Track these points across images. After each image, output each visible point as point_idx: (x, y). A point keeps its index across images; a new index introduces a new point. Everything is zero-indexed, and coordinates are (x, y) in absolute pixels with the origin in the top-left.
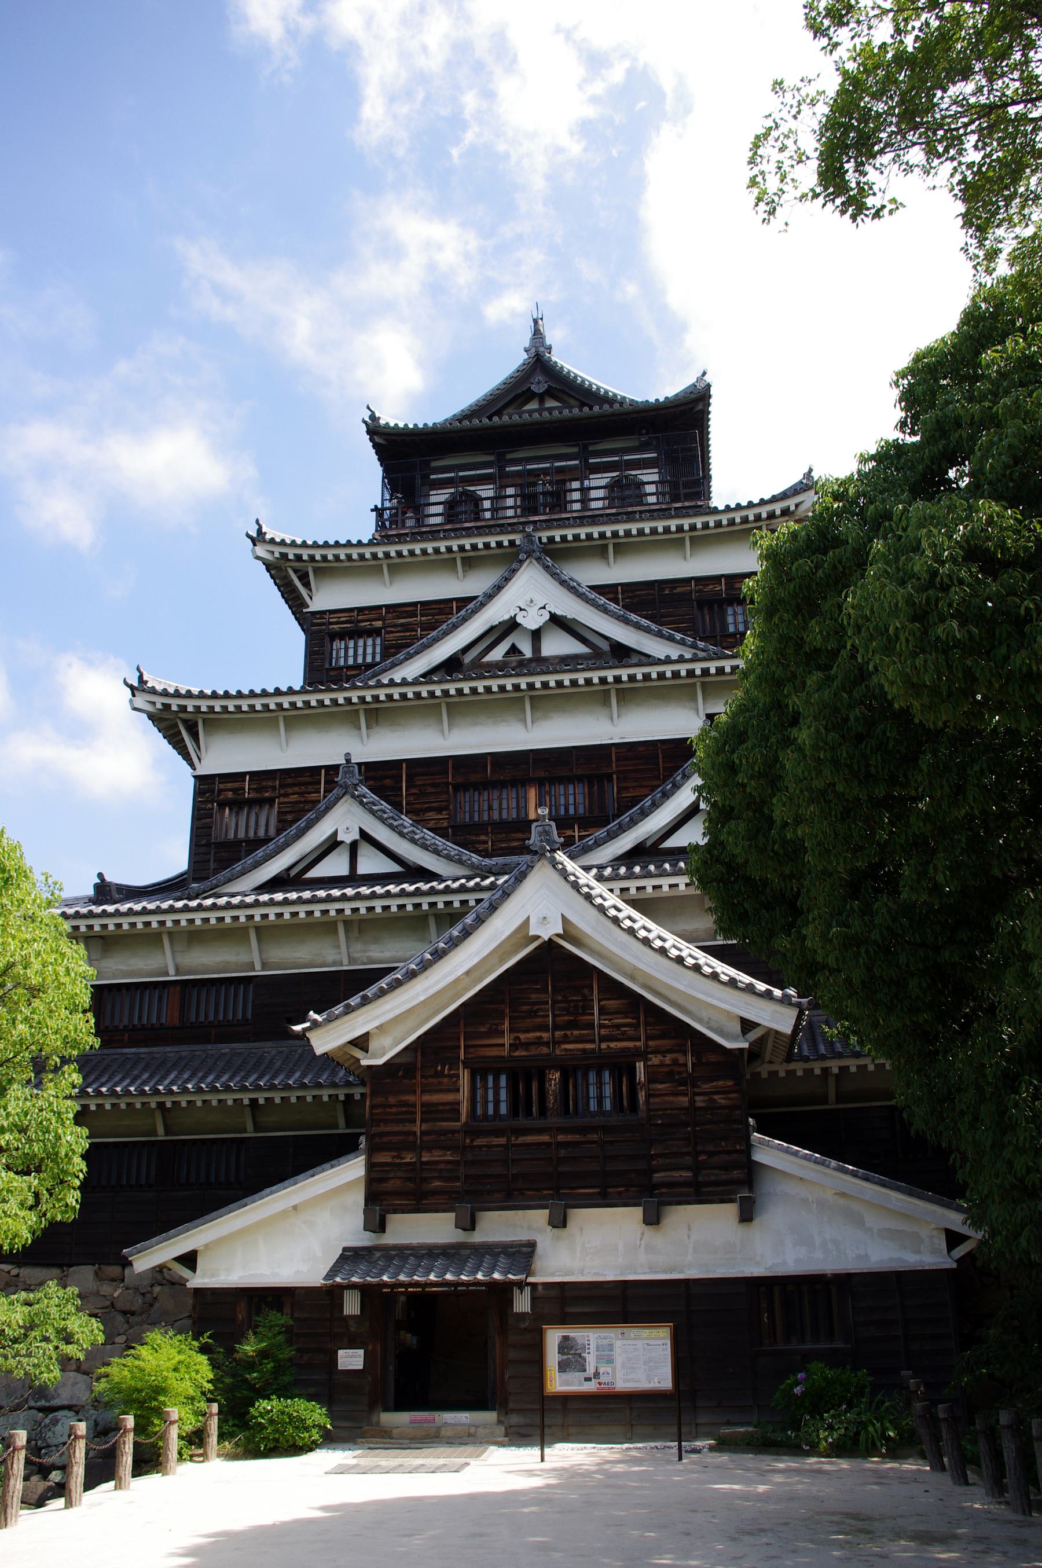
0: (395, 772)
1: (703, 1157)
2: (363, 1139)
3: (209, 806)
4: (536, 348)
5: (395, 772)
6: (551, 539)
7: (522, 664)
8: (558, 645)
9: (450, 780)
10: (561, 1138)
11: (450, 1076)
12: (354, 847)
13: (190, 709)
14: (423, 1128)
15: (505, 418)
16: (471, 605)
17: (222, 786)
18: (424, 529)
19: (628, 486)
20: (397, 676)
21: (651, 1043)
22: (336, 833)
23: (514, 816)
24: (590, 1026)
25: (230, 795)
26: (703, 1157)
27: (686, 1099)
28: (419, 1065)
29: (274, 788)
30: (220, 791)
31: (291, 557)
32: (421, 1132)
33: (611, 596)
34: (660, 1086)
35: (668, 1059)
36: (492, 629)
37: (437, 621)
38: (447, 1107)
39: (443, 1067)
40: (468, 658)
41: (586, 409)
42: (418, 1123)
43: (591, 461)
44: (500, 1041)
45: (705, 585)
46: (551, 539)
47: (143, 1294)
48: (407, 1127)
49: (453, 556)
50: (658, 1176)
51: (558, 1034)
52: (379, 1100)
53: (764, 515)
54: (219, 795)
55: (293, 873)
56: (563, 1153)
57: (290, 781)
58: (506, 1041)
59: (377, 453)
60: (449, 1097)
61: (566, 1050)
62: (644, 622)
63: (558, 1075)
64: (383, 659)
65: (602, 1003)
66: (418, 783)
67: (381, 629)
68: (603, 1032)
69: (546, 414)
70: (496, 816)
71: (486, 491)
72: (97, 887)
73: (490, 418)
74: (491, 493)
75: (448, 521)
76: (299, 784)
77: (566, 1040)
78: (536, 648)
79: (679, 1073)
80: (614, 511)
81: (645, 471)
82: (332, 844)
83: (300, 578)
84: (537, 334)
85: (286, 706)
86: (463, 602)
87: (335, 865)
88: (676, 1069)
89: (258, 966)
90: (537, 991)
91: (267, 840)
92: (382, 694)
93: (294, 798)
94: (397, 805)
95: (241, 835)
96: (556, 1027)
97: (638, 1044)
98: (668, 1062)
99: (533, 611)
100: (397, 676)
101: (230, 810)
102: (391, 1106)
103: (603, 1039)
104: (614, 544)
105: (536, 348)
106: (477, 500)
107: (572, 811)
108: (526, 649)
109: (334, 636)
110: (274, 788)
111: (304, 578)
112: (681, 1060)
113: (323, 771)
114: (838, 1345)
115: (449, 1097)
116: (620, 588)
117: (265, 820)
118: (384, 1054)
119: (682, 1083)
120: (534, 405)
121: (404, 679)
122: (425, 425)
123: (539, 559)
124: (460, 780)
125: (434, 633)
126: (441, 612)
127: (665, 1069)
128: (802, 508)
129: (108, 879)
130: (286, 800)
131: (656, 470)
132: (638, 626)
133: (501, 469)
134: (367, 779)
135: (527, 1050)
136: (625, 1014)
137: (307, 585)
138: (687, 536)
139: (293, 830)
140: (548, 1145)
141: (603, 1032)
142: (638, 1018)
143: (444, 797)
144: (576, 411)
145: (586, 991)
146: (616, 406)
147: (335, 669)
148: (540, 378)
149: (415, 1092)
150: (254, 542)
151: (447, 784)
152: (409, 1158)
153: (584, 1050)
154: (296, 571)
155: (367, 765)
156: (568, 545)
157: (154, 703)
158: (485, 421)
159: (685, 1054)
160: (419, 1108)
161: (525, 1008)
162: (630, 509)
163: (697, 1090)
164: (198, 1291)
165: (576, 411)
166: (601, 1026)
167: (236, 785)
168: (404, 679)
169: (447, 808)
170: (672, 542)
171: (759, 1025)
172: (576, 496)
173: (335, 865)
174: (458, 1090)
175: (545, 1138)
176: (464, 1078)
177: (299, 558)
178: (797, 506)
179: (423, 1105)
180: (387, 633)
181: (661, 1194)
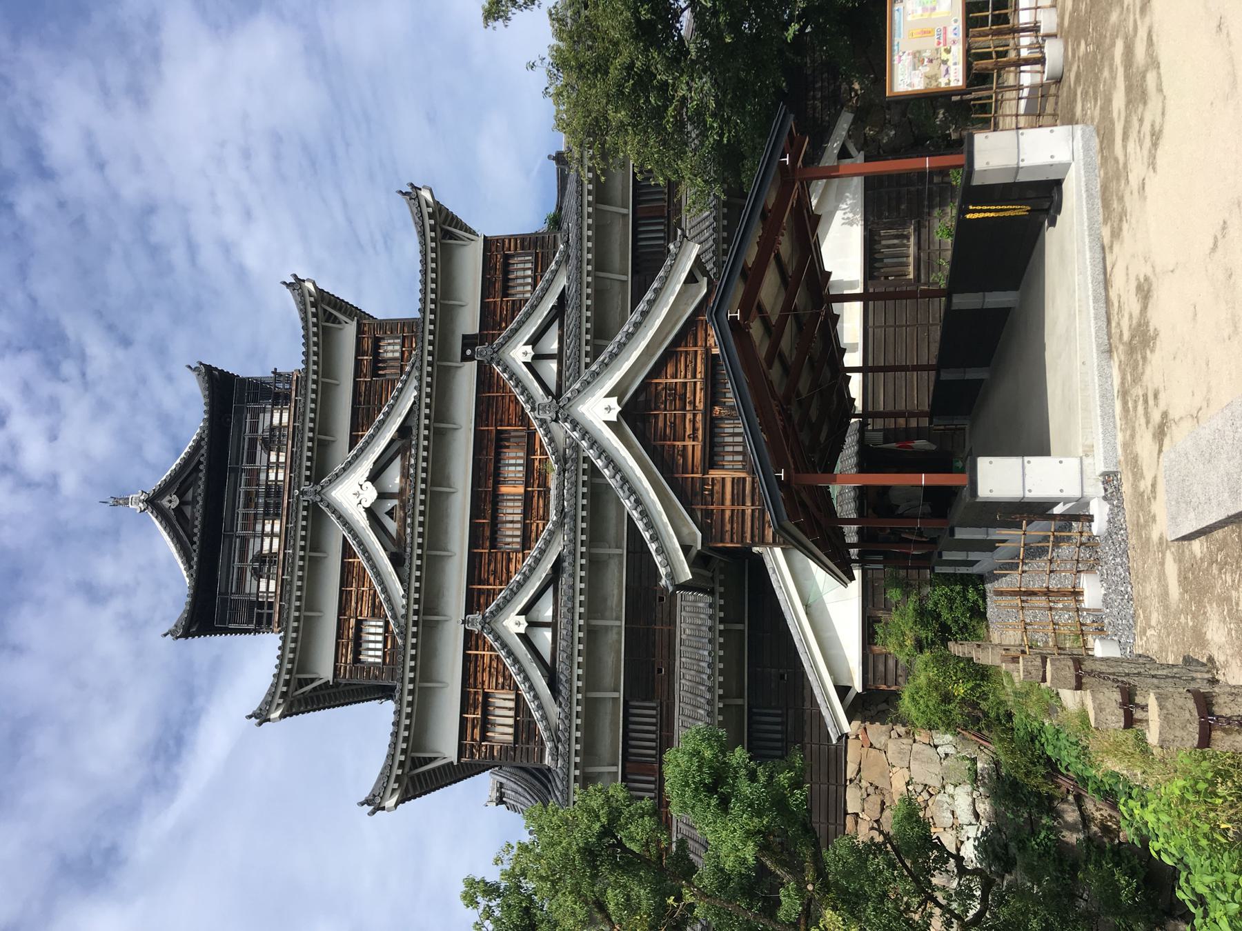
0: (475, 593)
2: (755, 549)
3: (483, 749)
5: (475, 593)
6: (308, 478)
7: (403, 506)
8: (393, 478)
9: (487, 551)
11: (713, 485)
13: (402, 758)
14: (749, 503)
15: (196, 530)
17: (469, 738)
18: (279, 592)
19: (272, 436)
21: (699, 344)
23: (519, 504)
25: (477, 731)
28: (704, 507)
29: (476, 693)
30: (473, 739)
31: (285, 689)
32: (752, 505)
37: (358, 574)
38: (736, 487)
39: (706, 490)
41: (201, 467)
44: (690, 449)
45: (362, 371)
46: (308, 478)
47: (868, 795)
49: (307, 558)
54: (476, 741)
57: (472, 680)
58: (689, 443)
61: (700, 402)
62: (385, 409)
63: (717, 408)
66: (486, 577)
67: (357, 620)
68: (689, 375)
69: (199, 499)
70: (518, 518)
73: (193, 543)
74: (258, 541)
76: (476, 672)
78: (391, 496)
80: (290, 442)
82: (524, 638)
83: (301, 687)
86: (347, 551)
87: (544, 638)
90: (656, 423)
91: (519, 699)
93: (486, 678)
94: (501, 590)
95: (511, 721)
96: (684, 408)
97: (699, 352)
102: (732, 528)
103: (694, 376)
105: (140, 501)
107: (521, 461)
109: (356, 660)
110: (476, 693)
111: (302, 683)
116: (354, 433)
117: (503, 702)
118: (695, 533)
120: (188, 510)
123: (323, 487)
124: (488, 544)
125: (368, 571)
126: (350, 572)
130: (486, 683)
131: (261, 415)
132: (387, 414)
135: (698, 430)
137: (313, 680)
138: (321, 379)
141: (689, 375)
143: (499, 555)
144: (201, 475)
145: (660, 388)
148: (165, 502)
151: (490, 553)
153: (701, 389)
154: (296, 690)
157: (394, 790)
158: (195, 547)
160: (736, 507)
161: (668, 431)
162: (291, 430)
166: (685, 377)
167: (469, 725)
169: (509, 553)
170: (326, 393)
173: (544, 638)
176: (715, 474)
177: (287, 683)
180: (361, 615)
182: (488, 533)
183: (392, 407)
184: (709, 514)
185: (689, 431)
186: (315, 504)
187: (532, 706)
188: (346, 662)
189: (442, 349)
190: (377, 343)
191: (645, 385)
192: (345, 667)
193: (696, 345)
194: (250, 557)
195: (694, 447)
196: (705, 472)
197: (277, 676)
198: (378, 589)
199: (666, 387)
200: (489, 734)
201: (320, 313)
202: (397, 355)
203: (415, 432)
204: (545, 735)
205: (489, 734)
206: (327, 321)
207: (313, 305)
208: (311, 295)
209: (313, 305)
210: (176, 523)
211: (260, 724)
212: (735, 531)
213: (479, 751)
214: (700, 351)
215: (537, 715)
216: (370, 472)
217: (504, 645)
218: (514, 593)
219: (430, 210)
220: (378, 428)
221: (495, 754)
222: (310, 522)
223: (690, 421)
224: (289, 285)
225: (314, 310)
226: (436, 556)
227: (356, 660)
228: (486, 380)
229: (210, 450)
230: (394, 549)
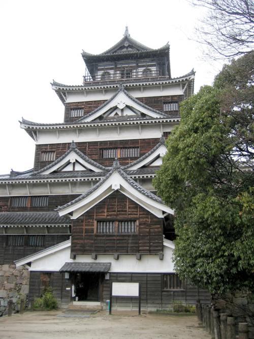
1: (152, 244)
2: (71, 237)
7: (118, 117)
8: (128, 113)
10: (118, 238)
12: (74, 164)
16: (106, 102)
20: (86, 121)
22: (69, 160)
24: (126, 211)
26: (152, 244)
34: (142, 226)
36: (111, 108)
40: (105, 116)
50: (140, 248)
52: (74, 228)
55: (59, 170)
56: (118, 242)
60: (92, 227)
63: (118, 223)
64: (84, 115)
71: (112, 72)
72: (11, 172)
74: (113, 73)
75: (102, 80)
77: (120, 214)
82: (69, 163)
83: (64, 94)
84: (127, 30)
87: (69, 168)
89: (50, 193)
91: (53, 162)
92: (82, 125)
94: (85, 153)
95: (47, 160)
96: (118, 211)
99: (122, 104)
100: (86, 121)
103: (129, 214)
106: (109, 74)
109: (71, 109)
111: (64, 94)
114: (182, 289)
115: (92, 227)
117: (52, 156)
123: (123, 91)
128: (191, 79)
129: (14, 170)
133: (116, 66)
134: (78, 146)
139: (59, 159)
145: (125, 203)
148: (126, 42)
150: (52, 85)
152: (82, 241)
164: (31, 271)
170: (157, 87)
171: (166, 212)
172: (135, 74)
174: (93, 226)
176: (95, 222)
177: (63, 89)
178: (189, 78)
182: (105, 147)
183: (151, 110)
184: (82, 222)
185: (110, 213)
186: (118, 89)
187: (48, 166)
191: (126, 197)
193: (140, 215)
195: (105, 215)
196: (96, 220)
197: (70, 86)
199: (125, 205)
203: (72, 123)
204: (39, 171)
207: (186, 80)
208: (189, 78)
209: (186, 80)
211: (51, 83)
217: (66, 156)
218: (82, 157)
224: (193, 71)
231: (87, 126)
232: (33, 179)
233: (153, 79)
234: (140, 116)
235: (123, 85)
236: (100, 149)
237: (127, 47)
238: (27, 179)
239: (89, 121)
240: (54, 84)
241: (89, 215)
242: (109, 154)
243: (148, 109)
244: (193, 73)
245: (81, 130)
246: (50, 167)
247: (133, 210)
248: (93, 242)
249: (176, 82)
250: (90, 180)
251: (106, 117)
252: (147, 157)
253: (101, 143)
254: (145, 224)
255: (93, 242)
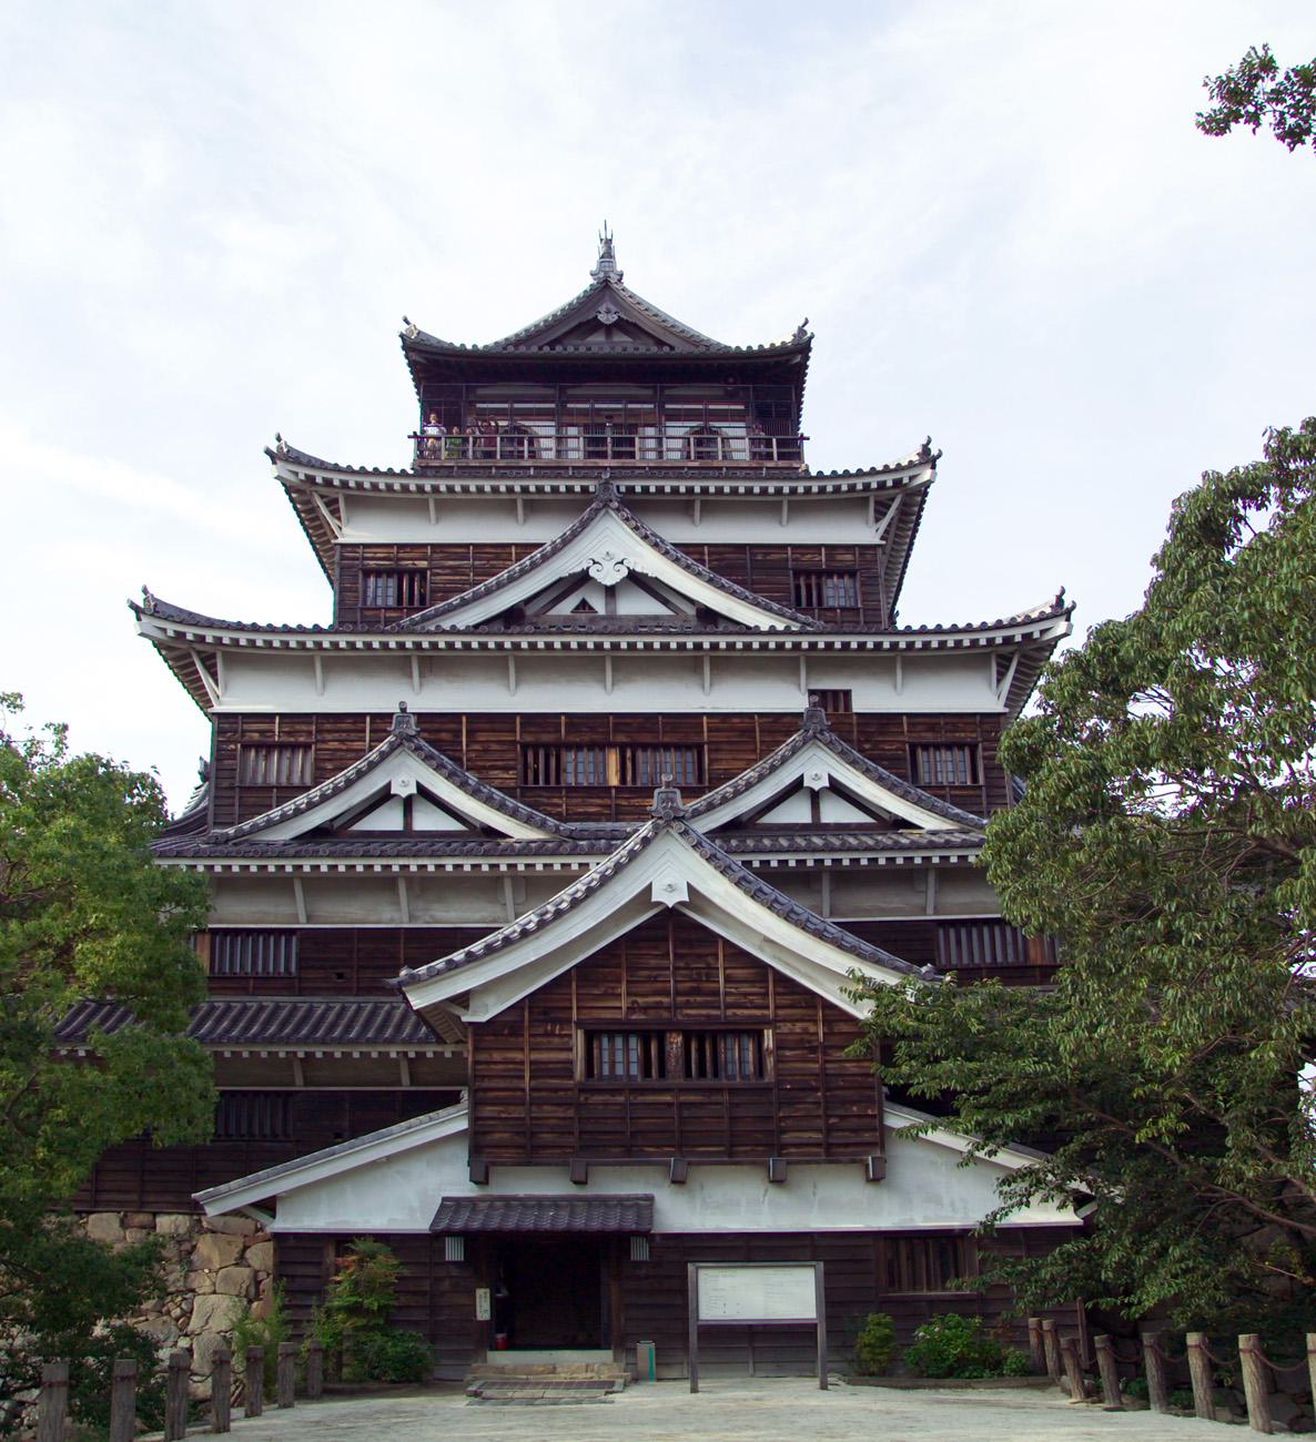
2: (465, 1095)
3: (233, 746)
4: (606, 272)
6: (631, 490)
8: (637, 605)
10: (683, 1098)
11: (560, 1036)
16: (537, 554)
17: (246, 727)
21: (780, 1012)
24: (716, 993)
25: (256, 736)
27: (817, 1066)
28: (526, 1024)
33: (696, 556)
35: (798, 1027)
36: (560, 579)
37: (493, 567)
41: (666, 349)
42: (527, 1079)
43: (668, 406)
44: (617, 1004)
45: (803, 554)
46: (631, 490)
48: (515, 1083)
49: (514, 497)
51: (680, 999)
53: (874, 486)
54: (243, 736)
57: (328, 726)
58: (624, 1003)
59: (412, 373)
60: (563, 1056)
63: (680, 1039)
65: (728, 971)
67: (426, 569)
68: (729, 999)
71: (544, 430)
77: (688, 1005)
79: (809, 1042)
81: (726, 424)
85: (326, 645)
86: (527, 548)
88: (806, 1037)
92: (442, 642)
96: (678, 993)
97: (765, 1012)
98: (798, 1031)
99: (608, 565)
101: (257, 753)
102: (495, 1063)
103: (728, 1006)
104: (702, 501)
108: (599, 605)
109: (367, 573)
110: (310, 733)
112: (812, 1029)
113: (368, 719)
115: (563, 1056)
118: (487, 1012)
119: (813, 1050)
121: (453, 627)
122: (474, 346)
123: (618, 510)
125: (492, 580)
127: (798, 1037)
131: (742, 424)
134: (423, 730)
136: (751, 982)
140: (669, 1105)
142: (767, 988)
146: (702, 349)
147: (369, 609)
149: (522, 1049)
152: (518, 1112)
153: (708, 1016)
155: (419, 715)
156: (650, 497)
159: (815, 1022)
160: (527, 1067)
163: (828, 1058)
165: (654, 349)
166: (726, 994)
168: (453, 627)
170: (766, 506)
174: (571, 1050)
175: (668, 1098)
176: (579, 1039)
178: (912, 478)
179: (531, 1063)
181: (789, 1154)
183: (745, 599)
188: (365, 559)
189: (819, 661)
190: (852, 574)
192: (357, 559)
194: (527, 423)
196: (579, 1024)
198: (468, 594)
200: (253, 753)
201: (886, 492)
202: (831, 603)
204: (246, 826)
205: (253, 753)
206: (876, 503)
207: (898, 483)
208: (912, 478)
209: (898, 483)
210: (579, 319)
212: (493, 1066)
213: (229, 742)
214: (770, 1012)
215: (275, 813)
216: (642, 574)
217: (372, 766)
219: (1036, 635)
220: (710, 581)
221: (226, 762)
222: (578, 497)
223: (657, 1003)
224: (926, 450)
225: (890, 484)
226: (507, 668)
227: (367, 573)
228: (777, 727)
229: (683, 358)
230: (530, 611)
231: (450, 646)
232: (227, 856)
233: (734, 472)
234: (694, 622)
235: (616, 483)
236: (525, 747)
237: (609, 329)
238: (197, 855)
239: (461, 627)
240: (282, 455)
241: (543, 1009)
242: (578, 768)
243: (734, 593)
244: (928, 458)
245: (435, 663)
246: (298, 812)
247: (746, 989)
248: (571, 1113)
249: (852, 488)
250: (503, 868)
251: (537, 615)
252: (749, 786)
253: (530, 720)
254: (799, 1044)
255: (571, 1113)
